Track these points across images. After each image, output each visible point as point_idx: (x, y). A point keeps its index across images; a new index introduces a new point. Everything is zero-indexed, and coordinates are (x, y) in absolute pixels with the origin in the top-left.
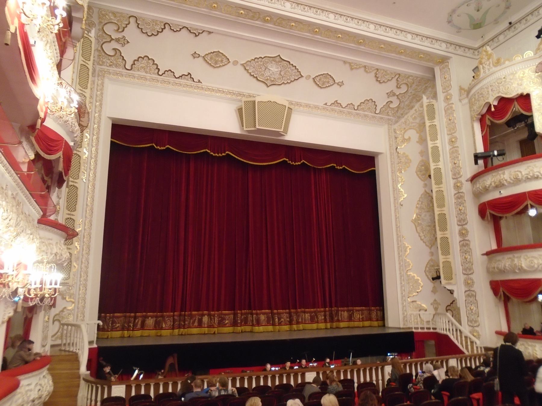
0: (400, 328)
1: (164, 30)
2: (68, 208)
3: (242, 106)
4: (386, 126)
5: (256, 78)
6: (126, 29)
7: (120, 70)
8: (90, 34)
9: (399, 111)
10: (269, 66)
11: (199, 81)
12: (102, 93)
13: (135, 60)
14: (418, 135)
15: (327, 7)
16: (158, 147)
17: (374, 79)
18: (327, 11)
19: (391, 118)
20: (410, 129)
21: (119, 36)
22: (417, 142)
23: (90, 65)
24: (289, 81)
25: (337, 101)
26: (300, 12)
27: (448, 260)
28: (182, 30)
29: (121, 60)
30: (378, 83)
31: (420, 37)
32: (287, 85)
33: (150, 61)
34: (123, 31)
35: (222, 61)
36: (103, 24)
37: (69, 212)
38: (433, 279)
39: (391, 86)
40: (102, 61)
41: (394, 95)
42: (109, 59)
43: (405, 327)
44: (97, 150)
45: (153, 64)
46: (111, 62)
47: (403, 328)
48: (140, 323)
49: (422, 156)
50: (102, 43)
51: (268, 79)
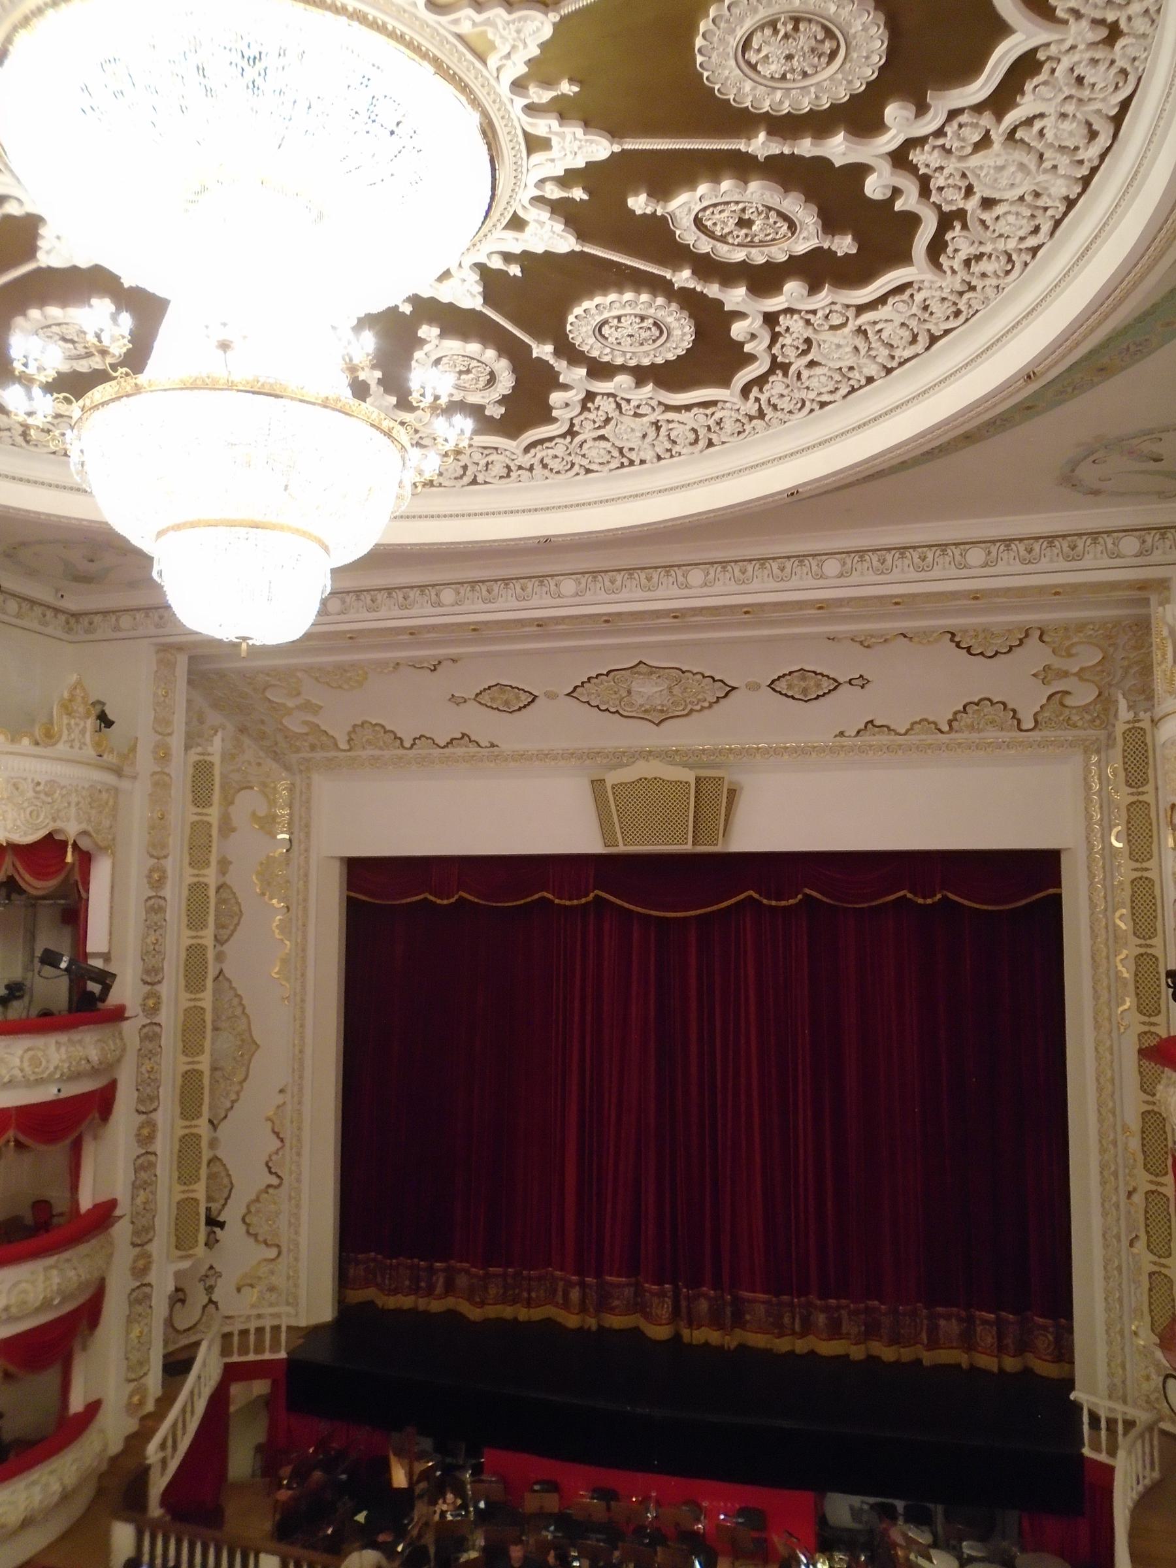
2: (184, 1116)
5: (617, 712)
7: (332, 754)
8: (210, 749)
10: (635, 687)
11: (493, 745)
12: (308, 809)
13: (349, 733)
15: (677, 558)
16: (439, 901)
18: (679, 566)
21: (300, 701)
24: (706, 704)
25: (871, 722)
26: (604, 597)
29: (324, 738)
31: (1022, 547)
32: (706, 712)
33: (377, 728)
35: (518, 698)
39: (1035, 655)
41: (1066, 674)
44: (305, 937)
45: (385, 732)
48: (441, 1280)
51: (646, 711)
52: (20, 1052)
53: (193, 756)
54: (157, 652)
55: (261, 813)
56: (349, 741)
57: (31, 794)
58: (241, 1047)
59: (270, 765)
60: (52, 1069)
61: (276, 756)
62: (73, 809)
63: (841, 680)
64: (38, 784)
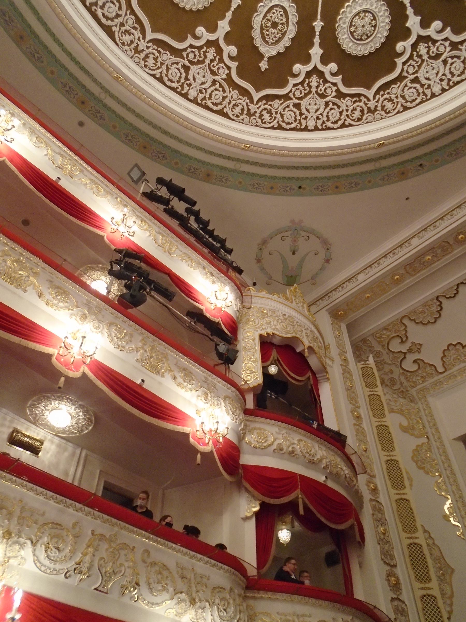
1: (443, 305)
6: (408, 335)
7: (436, 378)
12: (432, 416)
13: (442, 358)
23: (379, 390)
28: (460, 289)
29: (428, 368)
34: (407, 338)
36: (386, 345)
37: (422, 585)
40: (414, 382)
42: (417, 376)
46: (422, 377)
50: (399, 364)
52: (297, 439)
53: (360, 365)
54: (331, 317)
55: (405, 423)
56: (443, 364)
57: (281, 318)
58: (440, 569)
59: (401, 400)
60: (318, 457)
61: (403, 393)
62: (304, 334)
64: (285, 315)
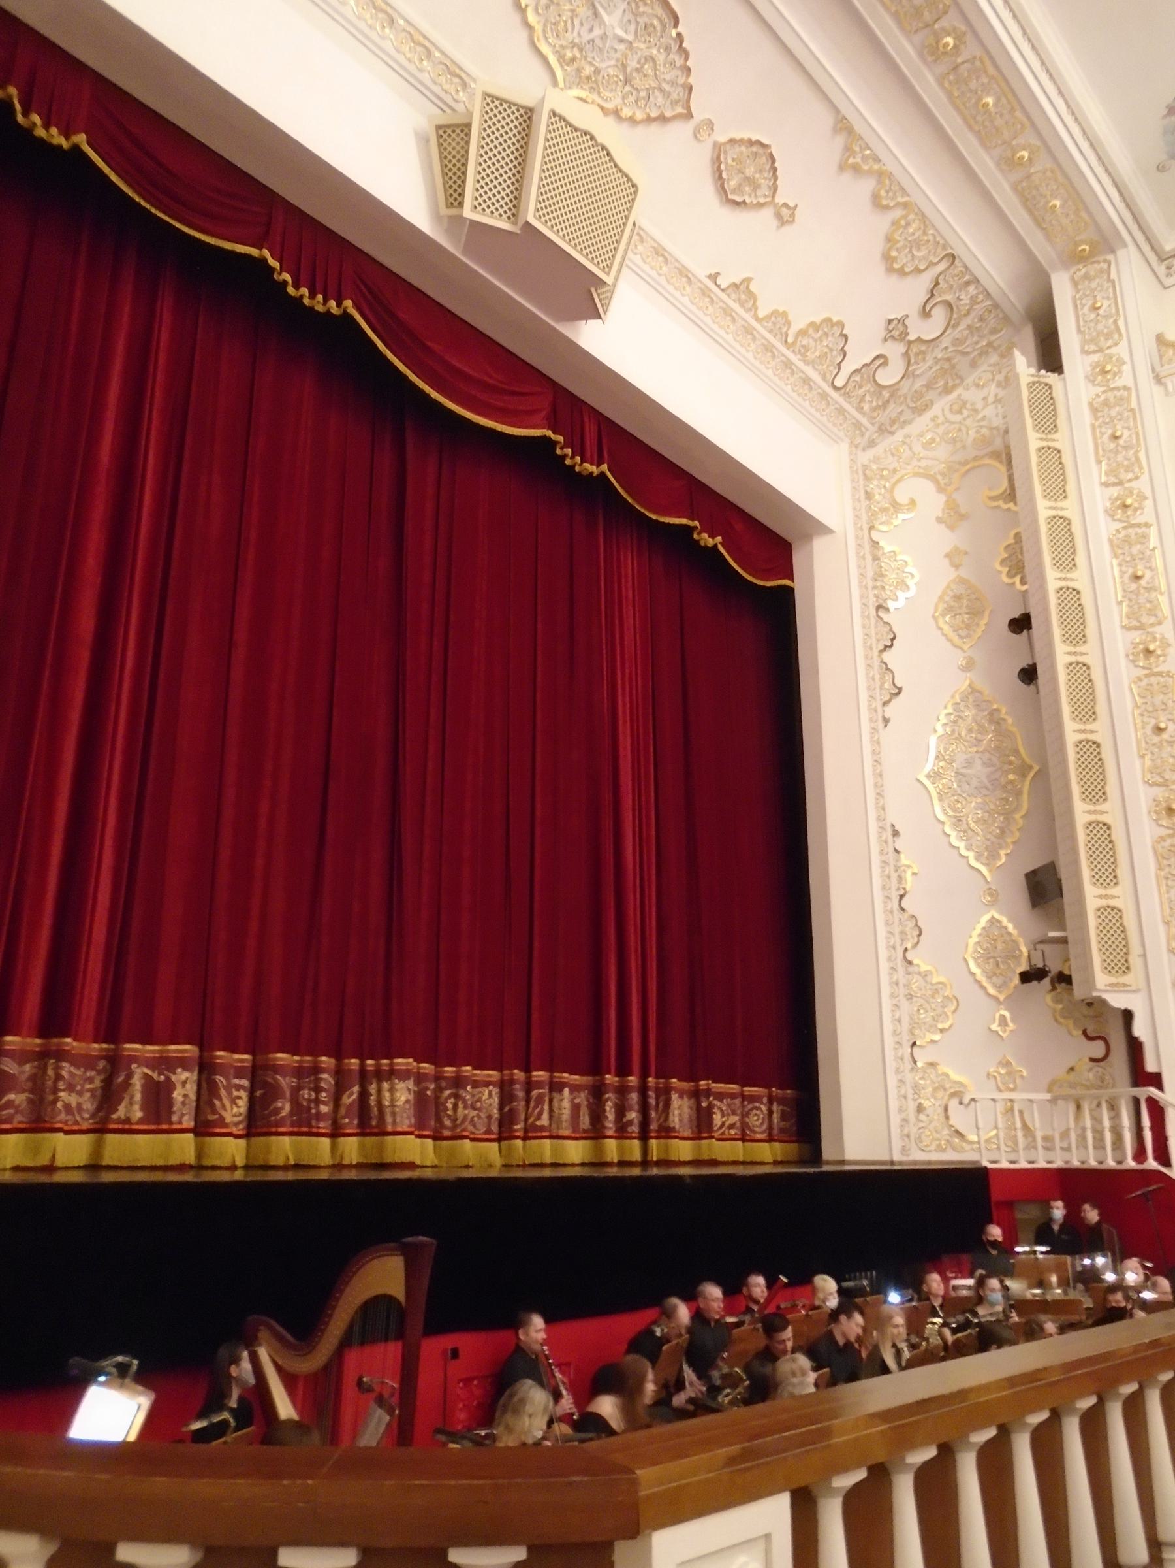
0: (892, 1163)
3: (471, 114)
4: (845, 446)
9: (892, 406)
14: (942, 498)
17: (879, 246)
19: (864, 421)
20: (917, 475)
22: (939, 520)
24: (639, 115)
25: (748, 280)
27: (1112, 903)
30: (881, 268)
38: (1026, 977)
43: (905, 1159)
47: (900, 1163)
49: (957, 567)
63: (780, 199)
